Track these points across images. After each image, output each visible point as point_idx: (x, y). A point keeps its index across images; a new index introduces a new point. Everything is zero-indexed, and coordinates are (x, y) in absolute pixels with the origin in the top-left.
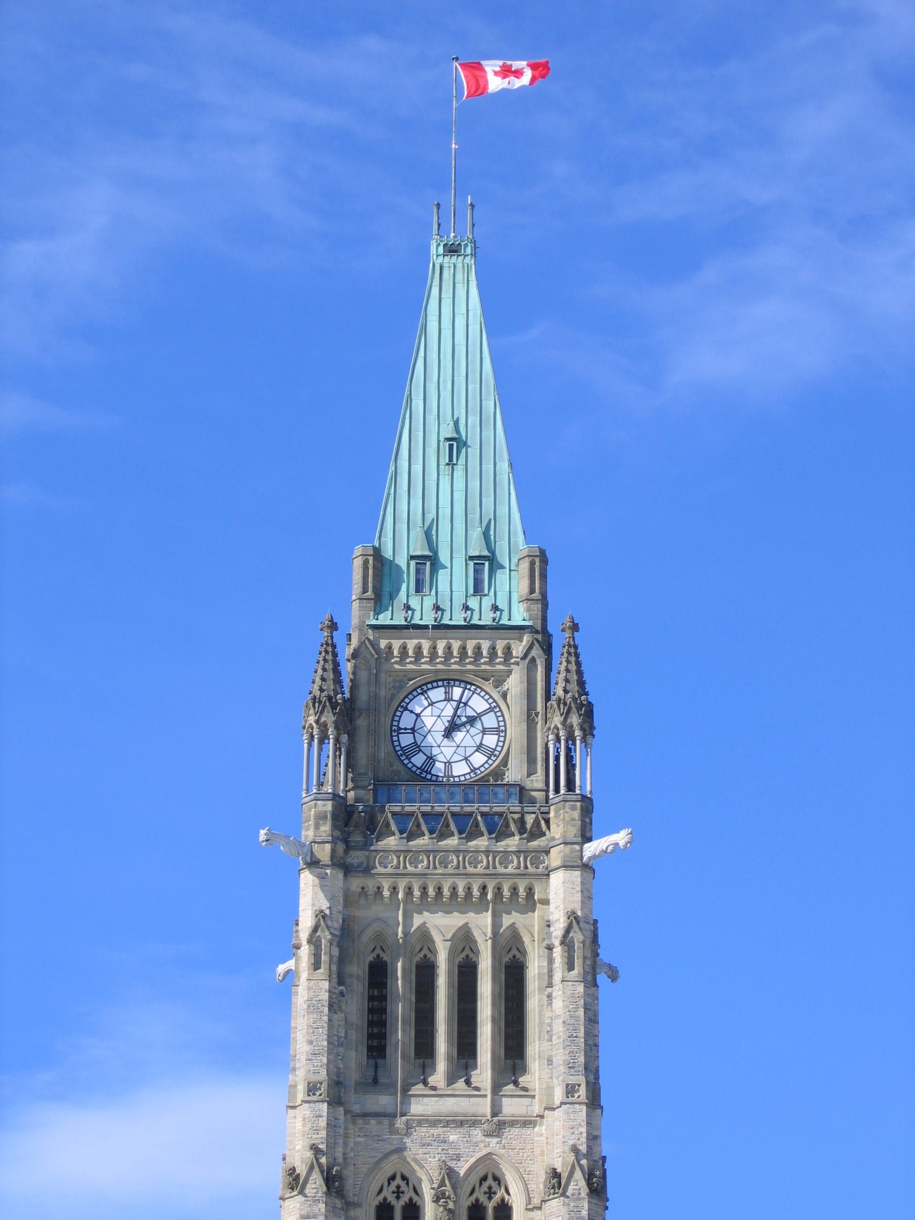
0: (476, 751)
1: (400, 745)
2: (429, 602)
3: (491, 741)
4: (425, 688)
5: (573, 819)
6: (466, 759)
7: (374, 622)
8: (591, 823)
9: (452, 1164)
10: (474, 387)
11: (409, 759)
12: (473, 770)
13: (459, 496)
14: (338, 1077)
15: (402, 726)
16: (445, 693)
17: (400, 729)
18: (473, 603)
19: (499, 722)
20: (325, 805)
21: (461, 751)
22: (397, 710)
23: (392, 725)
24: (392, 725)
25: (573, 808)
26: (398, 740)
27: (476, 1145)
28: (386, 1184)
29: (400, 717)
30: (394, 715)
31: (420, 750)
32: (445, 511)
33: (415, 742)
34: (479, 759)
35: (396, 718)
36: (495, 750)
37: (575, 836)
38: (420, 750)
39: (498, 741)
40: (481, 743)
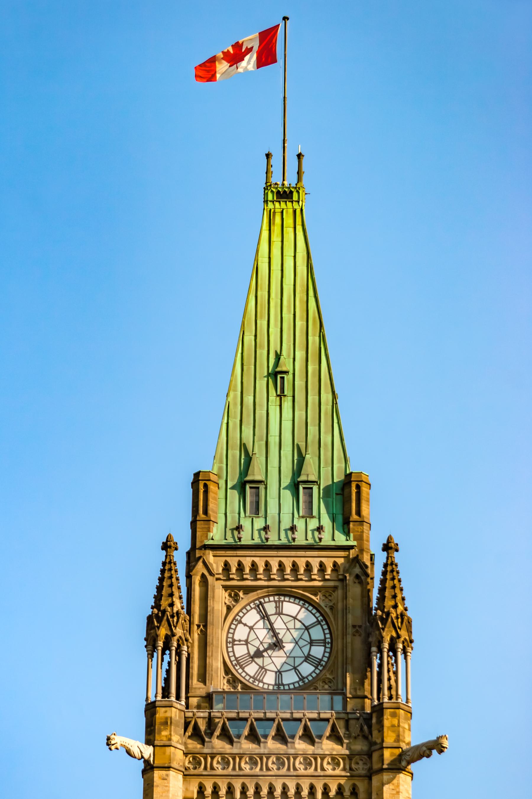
2: (259, 523)
3: (318, 651)
5: (393, 726)
6: (295, 668)
8: (410, 730)
10: (300, 324)
11: (243, 669)
12: (302, 679)
13: (287, 425)
15: (236, 637)
16: (276, 607)
17: (234, 640)
18: (300, 524)
19: (325, 634)
20: (166, 712)
23: (227, 637)
25: (394, 715)
29: (235, 630)
34: (307, 669)
35: (231, 631)
36: (321, 660)
37: (395, 741)
39: (325, 652)
40: (309, 654)
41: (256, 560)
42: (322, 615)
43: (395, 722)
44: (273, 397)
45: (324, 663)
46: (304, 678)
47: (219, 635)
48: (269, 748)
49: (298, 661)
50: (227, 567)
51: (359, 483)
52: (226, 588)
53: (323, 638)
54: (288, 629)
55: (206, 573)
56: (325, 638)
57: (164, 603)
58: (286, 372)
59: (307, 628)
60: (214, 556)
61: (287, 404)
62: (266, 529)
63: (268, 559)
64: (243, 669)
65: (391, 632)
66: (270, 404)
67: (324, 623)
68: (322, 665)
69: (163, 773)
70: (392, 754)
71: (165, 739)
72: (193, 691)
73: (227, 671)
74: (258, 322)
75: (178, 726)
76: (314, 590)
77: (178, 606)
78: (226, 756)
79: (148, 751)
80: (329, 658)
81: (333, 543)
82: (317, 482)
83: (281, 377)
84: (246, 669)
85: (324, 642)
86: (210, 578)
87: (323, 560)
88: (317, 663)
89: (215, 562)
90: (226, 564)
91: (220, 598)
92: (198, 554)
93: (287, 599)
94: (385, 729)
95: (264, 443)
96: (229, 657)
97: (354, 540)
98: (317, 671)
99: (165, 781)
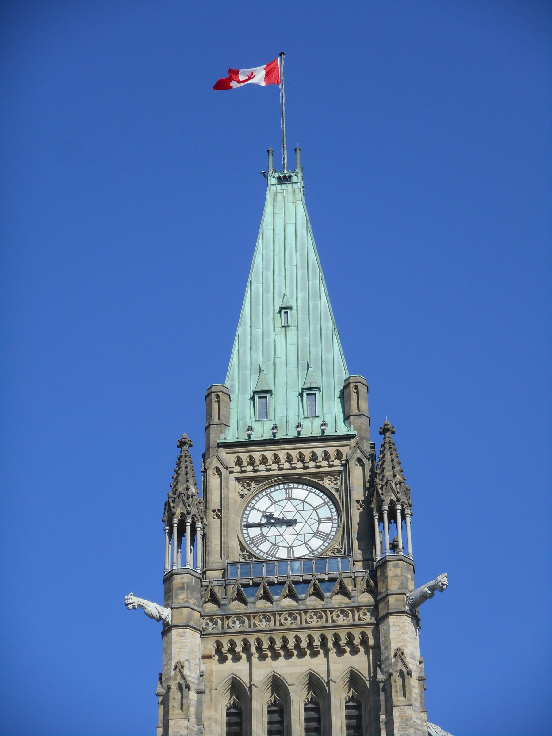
0: (314, 536)
1: (249, 536)
2: (268, 425)
3: (326, 528)
4: (269, 491)
5: (396, 576)
6: (305, 543)
7: (224, 441)
11: (257, 547)
13: (292, 349)
16: (286, 494)
18: (306, 423)
20: (182, 578)
21: (301, 537)
22: (245, 509)
23: (242, 522)
24: (242, 522)
25: (396, 566)
26: (248, 533)
29: (249, 515)
30: (244, 513)
31: (266, 539)
32: (281, 361)
33: (262, 533)
34: (316, 543)
35: (245, 516)
36: (329, 535)
37: (399, 589)
38: (266, 539)
41: (265, 453)
42: (328, 497)
43: (398, 572)
44: (278, 328)
45: (332, 537)
46: (314, 551)
47: (233, 519)
48: (281, 606)
49: (308, 537)
50: (239, 462)
51: (358, 384)
52: (238, 479)
53: (330, 516)
54: (298, 511)
55: (220, 467)
56: (332, 516)
58: (291, 308)
59: (315, 509)
60: (227, 453)
61: (291, 332)
63: (276, 452)
64: (257, 547)
65: (391, 496)
66: (276, 333)
67: (331, 503)
68: (330, 539)
69: (181, 631)
70: (398, 600)
71: (181, 601)
73: (243, 549)
74: (264, 273)
75: (195, 591)
76: (321, 476)
77: (193, 490)
78: (241, 615)
79: (166, 613)
80: (336, 532)
81: (336, 434)
82: (319, 388)
84: (260, 547)
85: (331, 519)
86: (223, 470)
87: (327, 449)
88: (325, 537)
89: (229, 458)
90: (239, 459)
91: (234, 487)
93: (296, 485)
94: (389, 579)
95: (271, 363)
96: (244, 538)
97: (354, 431)
98: (326, 544)
99: (183, 638)
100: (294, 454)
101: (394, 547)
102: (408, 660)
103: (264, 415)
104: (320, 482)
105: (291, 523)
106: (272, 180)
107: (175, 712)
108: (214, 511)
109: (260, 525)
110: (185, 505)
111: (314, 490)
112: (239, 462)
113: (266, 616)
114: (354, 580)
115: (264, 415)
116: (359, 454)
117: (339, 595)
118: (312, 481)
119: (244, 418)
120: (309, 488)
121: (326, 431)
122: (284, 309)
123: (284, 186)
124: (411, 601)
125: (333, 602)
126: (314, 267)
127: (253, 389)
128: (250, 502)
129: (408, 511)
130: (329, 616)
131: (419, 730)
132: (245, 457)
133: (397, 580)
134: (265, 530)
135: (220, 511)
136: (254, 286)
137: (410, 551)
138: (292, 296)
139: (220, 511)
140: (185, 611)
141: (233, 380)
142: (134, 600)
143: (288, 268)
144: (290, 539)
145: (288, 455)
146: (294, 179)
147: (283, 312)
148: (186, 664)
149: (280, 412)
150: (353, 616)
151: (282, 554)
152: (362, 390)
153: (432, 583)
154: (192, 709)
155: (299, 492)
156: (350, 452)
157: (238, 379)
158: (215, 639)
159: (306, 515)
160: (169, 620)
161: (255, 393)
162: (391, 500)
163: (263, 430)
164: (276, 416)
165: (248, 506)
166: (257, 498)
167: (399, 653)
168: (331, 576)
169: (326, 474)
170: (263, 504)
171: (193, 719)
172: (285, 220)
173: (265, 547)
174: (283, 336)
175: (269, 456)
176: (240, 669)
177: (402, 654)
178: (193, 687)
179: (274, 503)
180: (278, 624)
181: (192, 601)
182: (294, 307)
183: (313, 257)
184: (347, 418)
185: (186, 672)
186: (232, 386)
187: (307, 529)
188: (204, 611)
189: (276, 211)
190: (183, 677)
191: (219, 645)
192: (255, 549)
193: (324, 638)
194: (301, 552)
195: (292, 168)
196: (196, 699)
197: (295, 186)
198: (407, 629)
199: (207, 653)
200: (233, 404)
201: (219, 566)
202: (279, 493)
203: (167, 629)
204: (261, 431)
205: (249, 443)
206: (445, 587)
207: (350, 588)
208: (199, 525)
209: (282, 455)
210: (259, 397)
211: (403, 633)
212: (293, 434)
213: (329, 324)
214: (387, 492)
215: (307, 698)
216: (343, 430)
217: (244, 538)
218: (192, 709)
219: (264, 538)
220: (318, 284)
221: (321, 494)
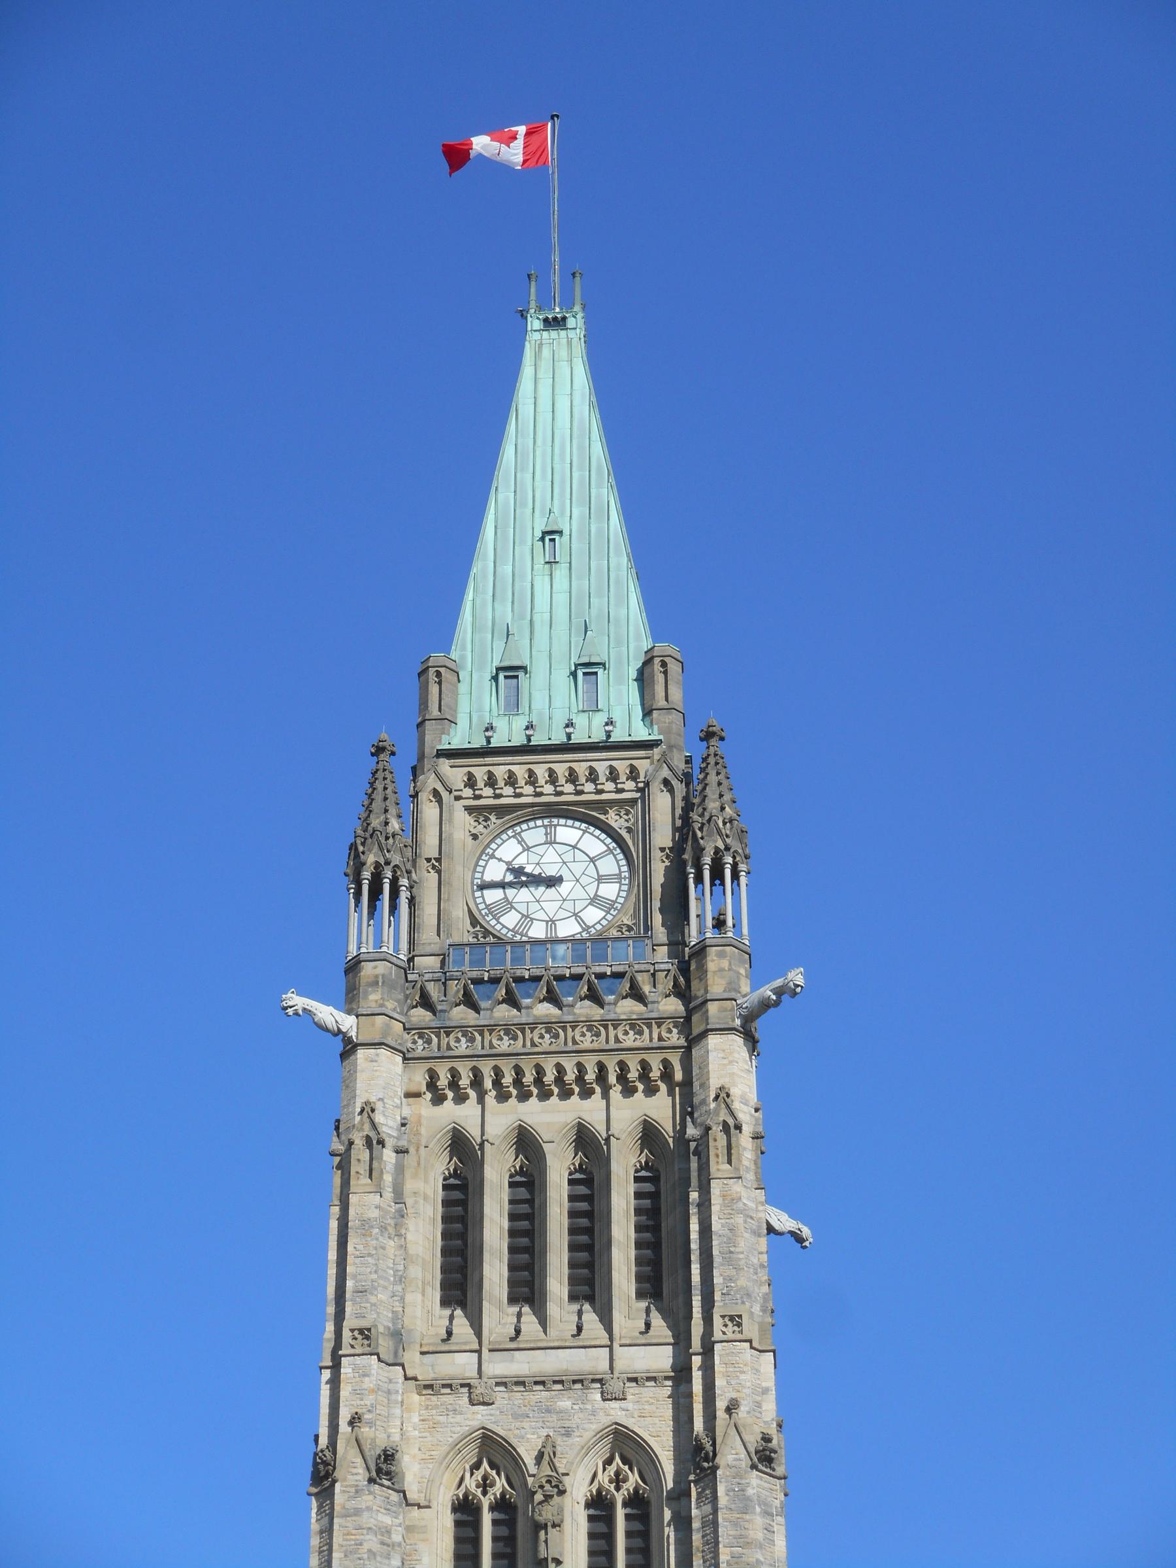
1: (484, 902)
2: (520, 722)
3: (610, 891)
4: (518, 829)
5: (722, 970)
6: (576, 915)
9: (559, 1441)
13: (561, 599)
14: (394, 1323)
16: (546, 834)
18: (581, 721)
20: (375, 967)
21: (568, 905)
22: (479, 858)
23: (473, 878)
24: (473, 878)
25: (721, 955)
26: (482, 896)
27: (594, 1413)
28: (468, 1475)
29: (484, 867)
30: (477, 865)
31: (512, 907)
32: (541, 618)
34: (593, 915)
35: (479, 869)
36: (615, 902)
40: (596, 895)
41: (513, 768)
42: (614, 840)
43: (725, 964)
47: (459, 873)
50: (471, 782)
51: (666, 659)
52: (469, 810)
54: (564, 863)
55: (440, 789)
56: (621, 872)
57: (376, 822)
58: (560, 533)
59: (593, 860)
61: (561, 572)
62: (530, 726)
67: (618, 851)
69: (371, 1052)
71: (373, 1005)
72: (421, 947)
73: (474, 922)
74: (518, 475)
76: (603, 806)
77: (395, 825)
79: (348, 1023)
82: (604, 664)
83: (551, 540)
85: (618, 877)
86: (445, 795)
87: (613, 763)
88: (608, 906)
89: (455, 774)
91: (462, 822)
92: (427, 764)
93: (562, 821)
94: (709, 975)
96: (477, 905)
98: (609, 917)
100: (561, 770)
101: (719, 924)
102: (736, 1105)
103: (514, 705)
104: (602, 817)
105: (553, 882)
106: (535, 323)
107: (360, 1181)
108: (429, 860)
109: (502, 885)
110: (381, 849)
111: (592, 829)
112: (471, 782)
113: (509, 1031)
114: (653, 975)
115: (514, 705)
116: (665, 773)
117: (504, 1005)
118: (588, 815)
119: (480, 710)
120: (584, 826)
121: (492, 740)
122: (550, 534)
123: (554, 334)
124: (744, 1012)
125: (618, 1010)
126: (599, 467)
127: (496, 663)
128: (488, 846)
129: (742, 867)
130: (444, 1041)
131: (752, 1218)
132: (480, 774)
133: (723, 977)
134: (511, 892)
135: (438, 860)
136: (501, 496)
137: (745, 931)
138: (562, 513)
139: (438, 860)
140: (380, 1020)
141: (464, 648)
142: (297, 1001)
143: (557, 467)
144: (551, 908)
145: (551, 773)
146: (571, 322)
147: (547, 538)
148: (379, 1106)
149: (540, 702)
150: (439, 1041)
151: (538, 931)
152: (674, 668)
153: (778, 983)
154: (388, 1178)
155: (568, 832)
156: (651, 769)
157: (473, 648)
158: (427, 1065)
159: (577, 869)
160: (353, 1034)
161: (498, 669)
162: (717, 848)
163: (510, 729)
164: (533, 707)
165: (485, 853)
166: (499, 841)
167: (723, 1095)
168: (615, 969)
169: (612, 803)
170: (509, 850)
171: (388, 1194)
172: (555, 388)
173: (510, 920)
174: (547, 578)
175: (520, 772)
176: (467, 1115)
177: (728, 1096)
178: (390, 1143)
179: (527, 849)
180: (528, 1044)
181: (390, 1005)
182: (566, 532)
183: (598, 450)
184: (647, 713)
185: (379, 1118)
186: (463, 657)
187: (579, 893)
188: (410, 1021)
189: (540, 375)
190: (374, 1126)
191: (433, 1076)
192: (493, 922)
193: (602, 1067)
194: (568, 929)
195: (568, 304)
196: (394, 1161)
197: (571, 334)
198: (736, 1055)
199: (414, 1088)
200: (463, 688)
201: (435, 949)
202: (534, 833)
203: (349, 1048)
204: (509, 733)
205: (488, 751)
206: (798, 990)
207: (647, 989)
208: (404, 881)
209: (541, 772)
210: (506, 677)
211: (731, 1062)
212: (559, 738)
213: (621, 561)
214: (710, 835)
215: (448, 1169)
216: (641, 733)
217: (477, 905)
218: (388, 1178)
219: (509, 905)
220: (606, 495)
221: (603, 836)
